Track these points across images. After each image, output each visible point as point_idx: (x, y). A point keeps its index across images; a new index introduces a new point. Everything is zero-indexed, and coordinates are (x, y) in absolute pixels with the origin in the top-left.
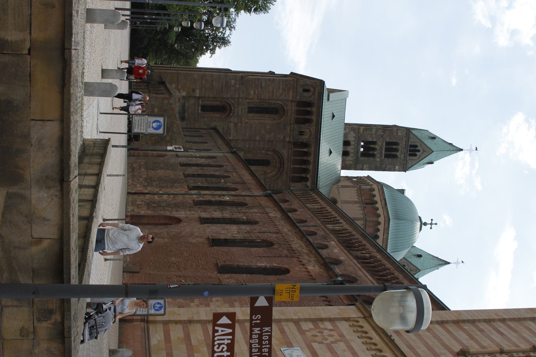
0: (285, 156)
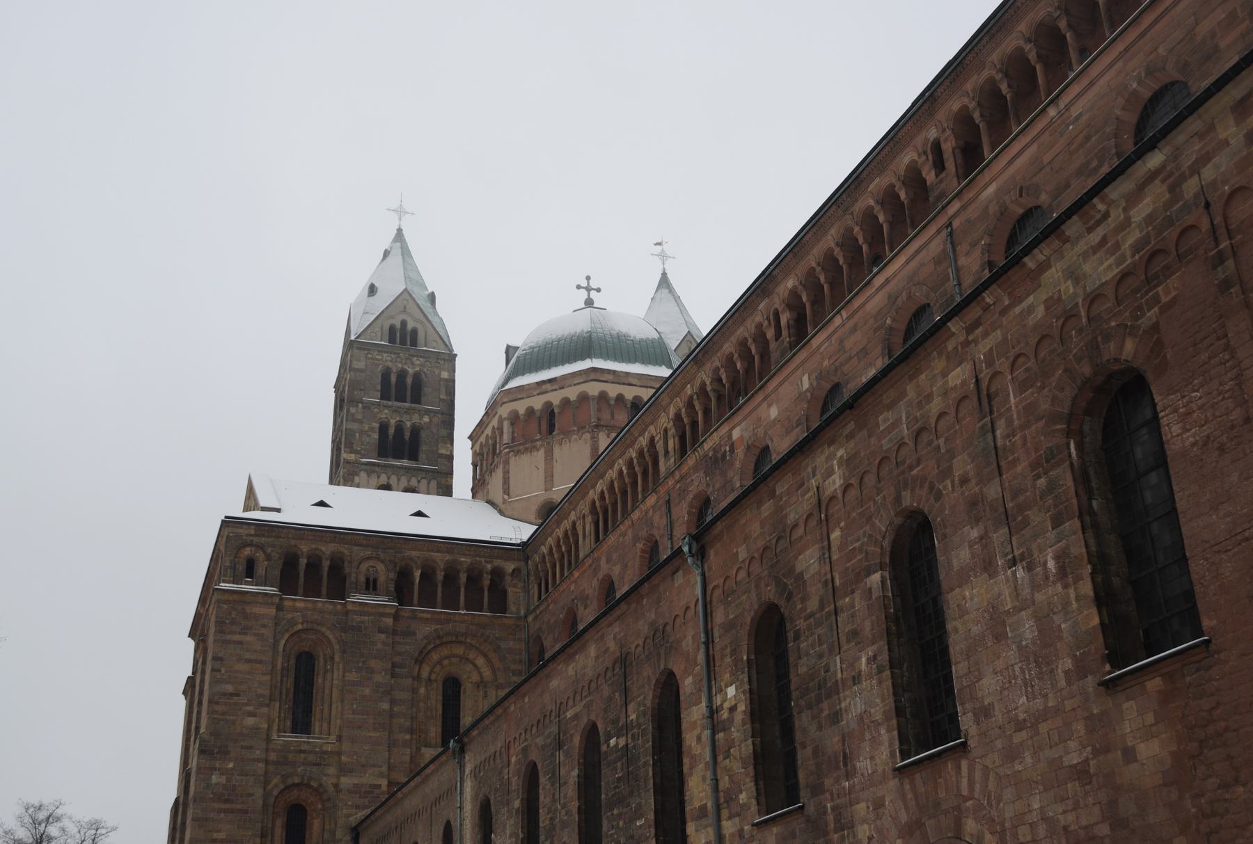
0: (436, 630)
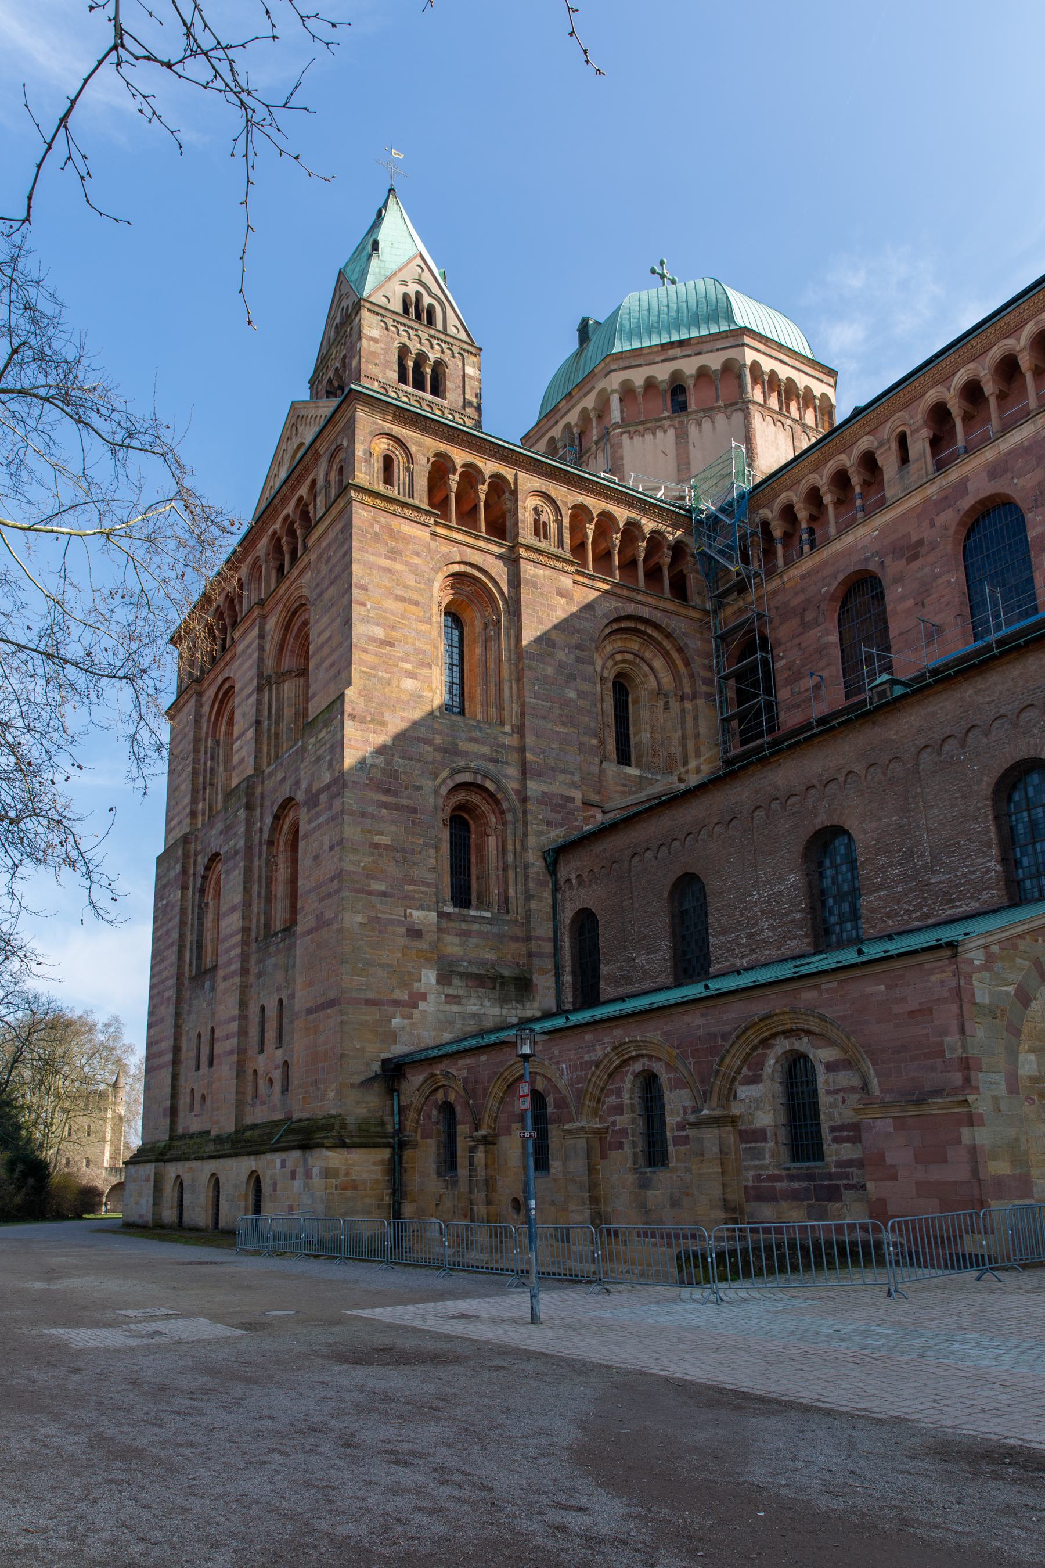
0: (616, 608)
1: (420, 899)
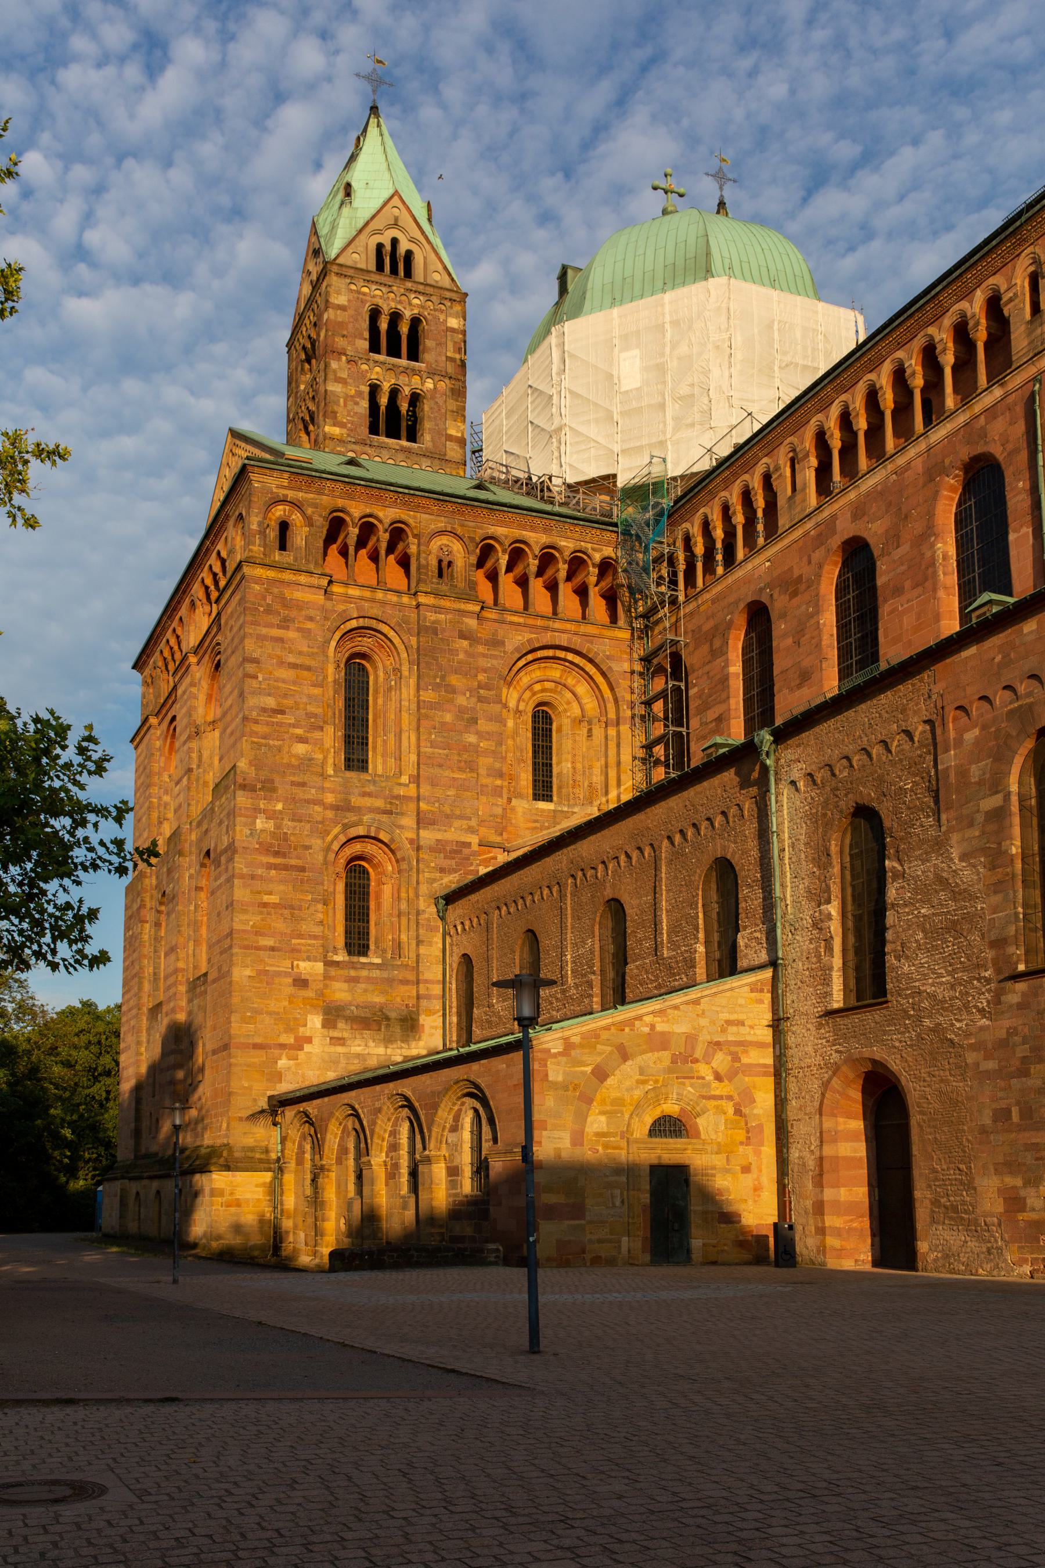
1: (308, 951)
